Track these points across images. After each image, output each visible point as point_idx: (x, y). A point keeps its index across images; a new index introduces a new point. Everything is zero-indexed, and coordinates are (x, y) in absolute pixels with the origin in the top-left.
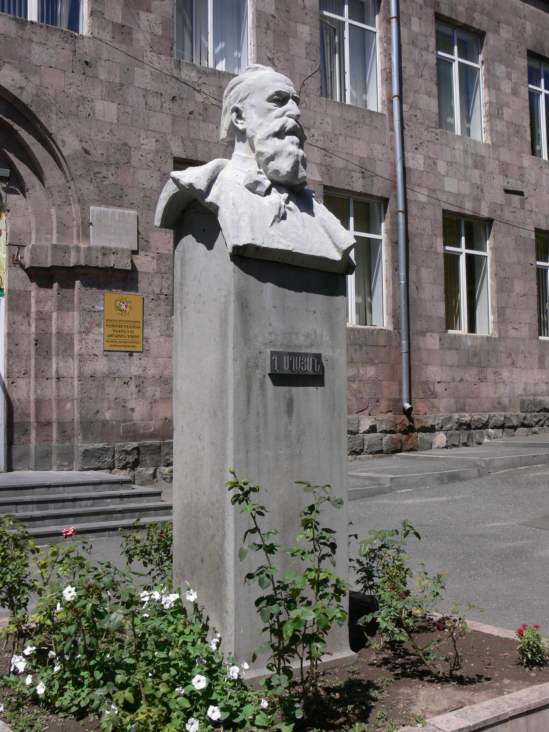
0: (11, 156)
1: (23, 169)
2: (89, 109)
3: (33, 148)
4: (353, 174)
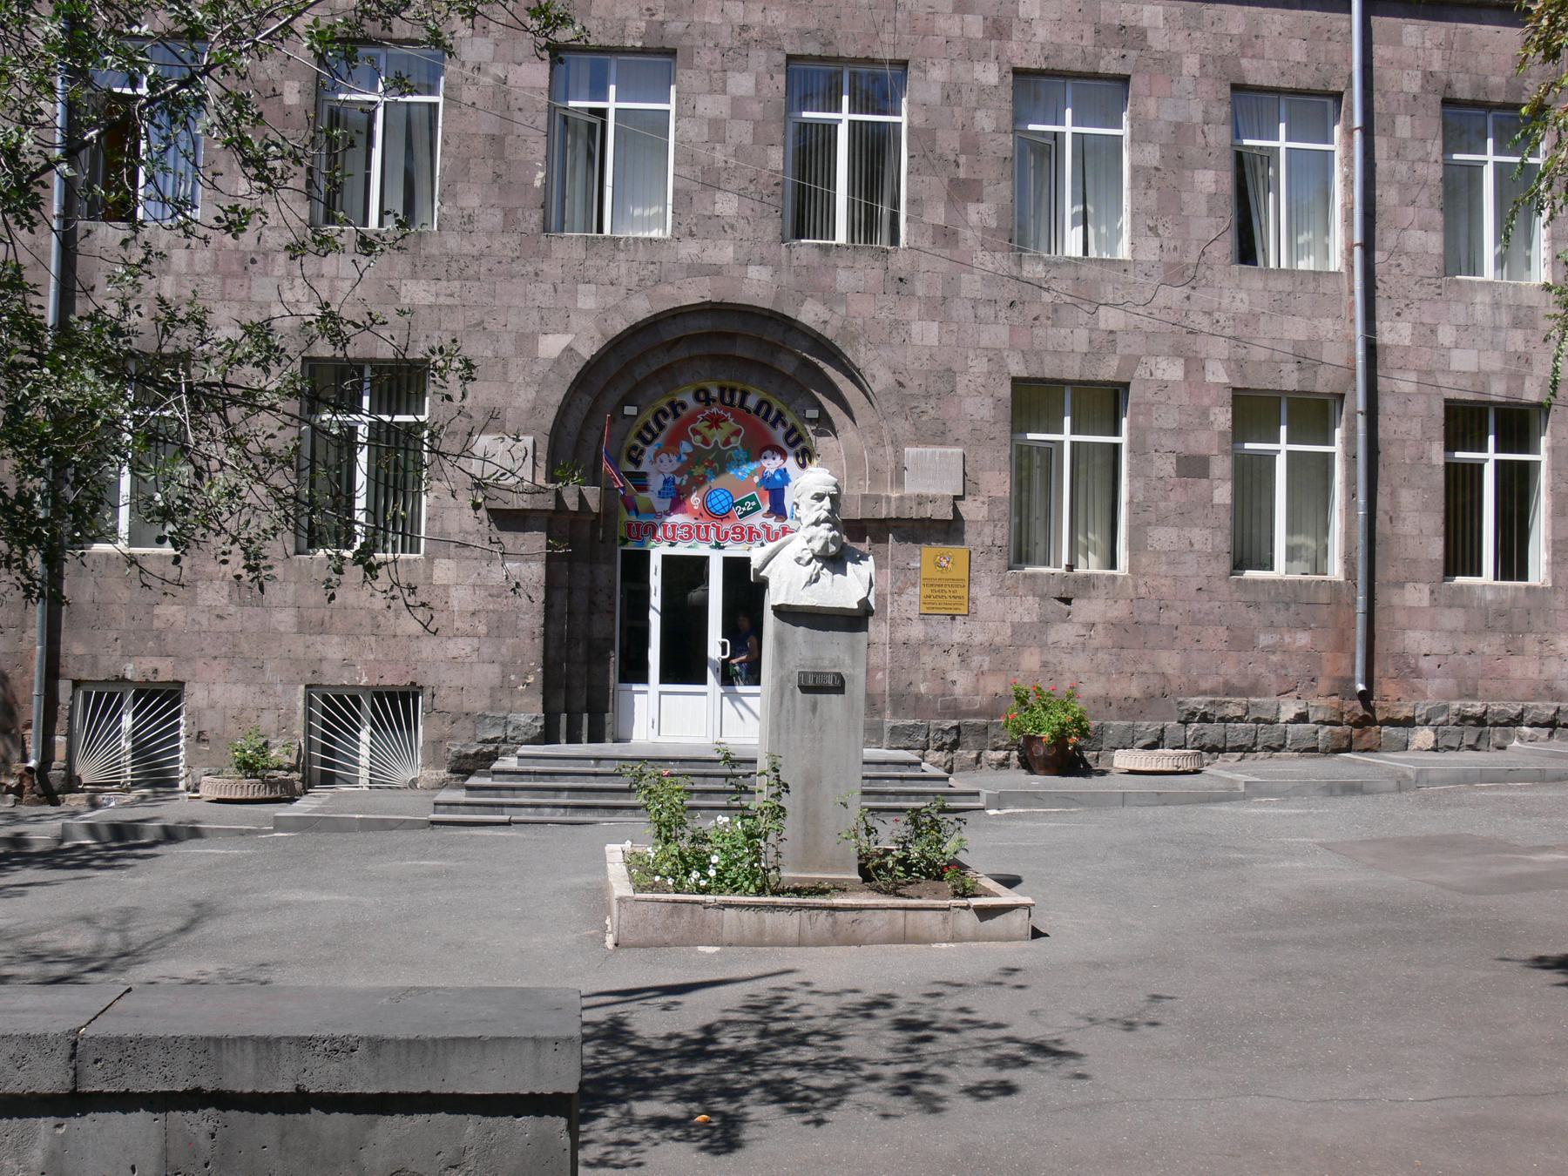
0: (820, 396)
1: (832, 408)
3: (840, 386)
4: (1283, 366)
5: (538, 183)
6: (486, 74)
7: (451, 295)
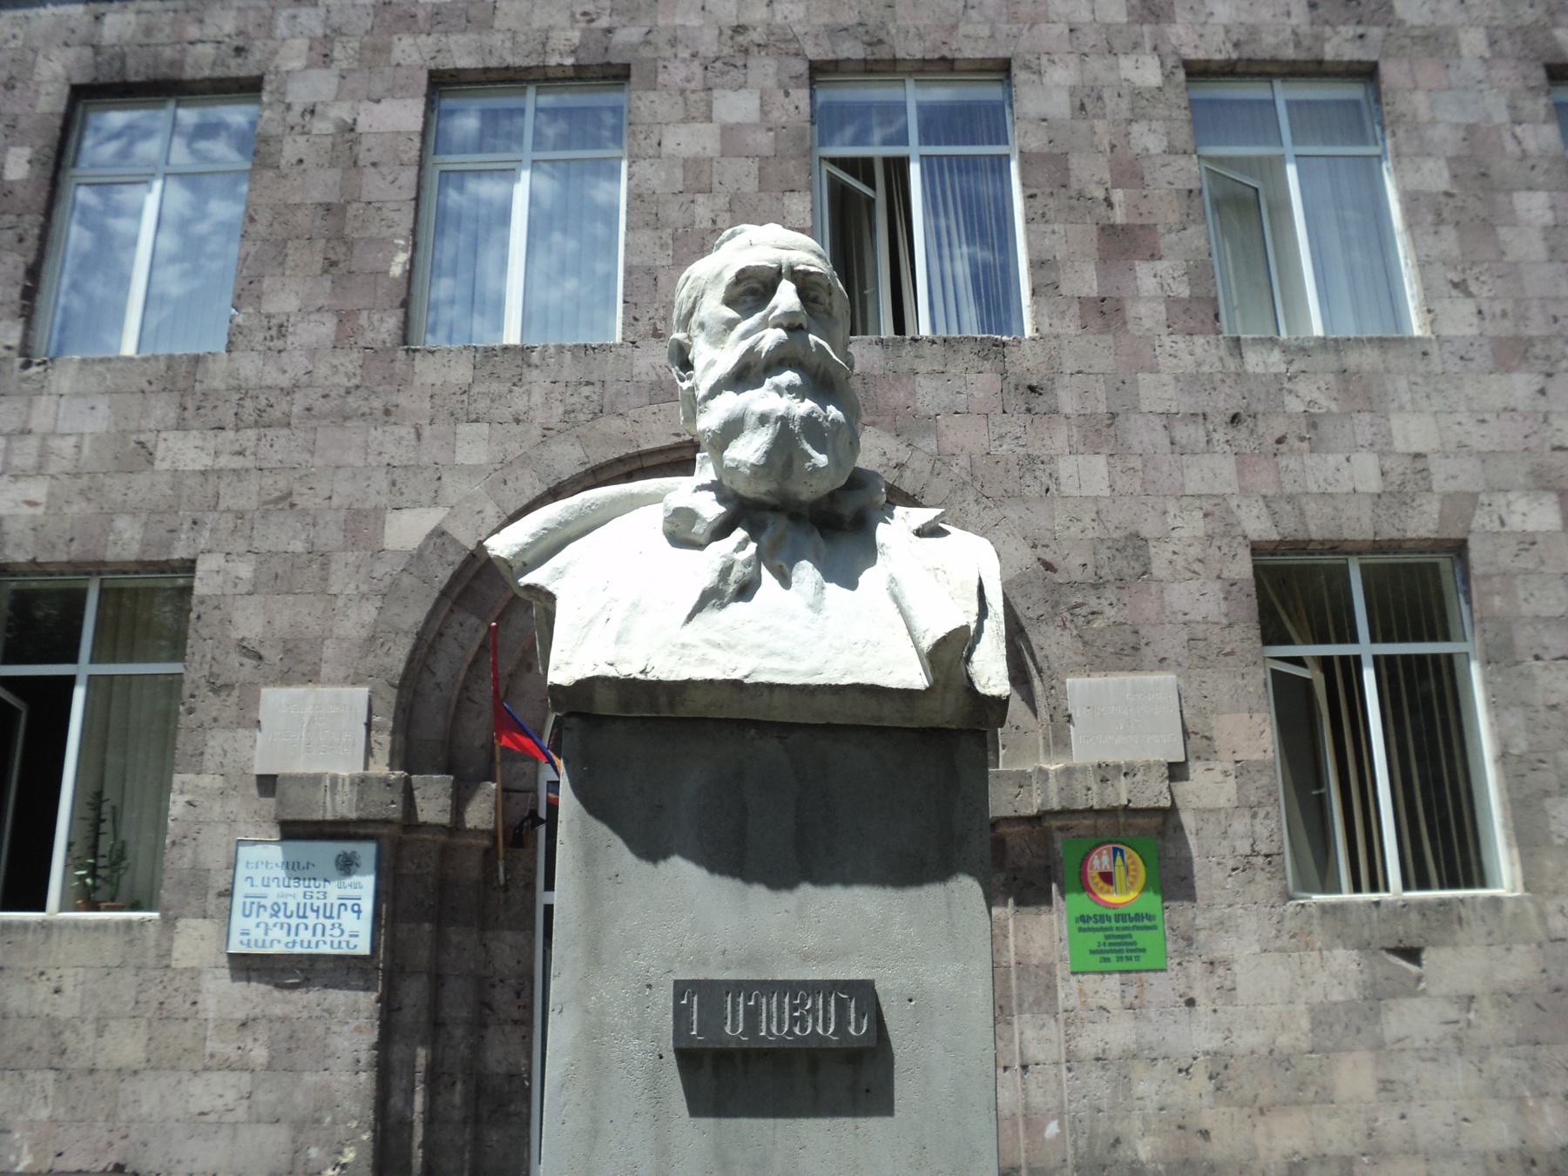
2: (1045, 479)
5: (396, 270)
6: (324, 117)
7: (241, 453)
